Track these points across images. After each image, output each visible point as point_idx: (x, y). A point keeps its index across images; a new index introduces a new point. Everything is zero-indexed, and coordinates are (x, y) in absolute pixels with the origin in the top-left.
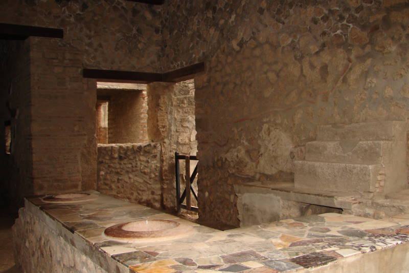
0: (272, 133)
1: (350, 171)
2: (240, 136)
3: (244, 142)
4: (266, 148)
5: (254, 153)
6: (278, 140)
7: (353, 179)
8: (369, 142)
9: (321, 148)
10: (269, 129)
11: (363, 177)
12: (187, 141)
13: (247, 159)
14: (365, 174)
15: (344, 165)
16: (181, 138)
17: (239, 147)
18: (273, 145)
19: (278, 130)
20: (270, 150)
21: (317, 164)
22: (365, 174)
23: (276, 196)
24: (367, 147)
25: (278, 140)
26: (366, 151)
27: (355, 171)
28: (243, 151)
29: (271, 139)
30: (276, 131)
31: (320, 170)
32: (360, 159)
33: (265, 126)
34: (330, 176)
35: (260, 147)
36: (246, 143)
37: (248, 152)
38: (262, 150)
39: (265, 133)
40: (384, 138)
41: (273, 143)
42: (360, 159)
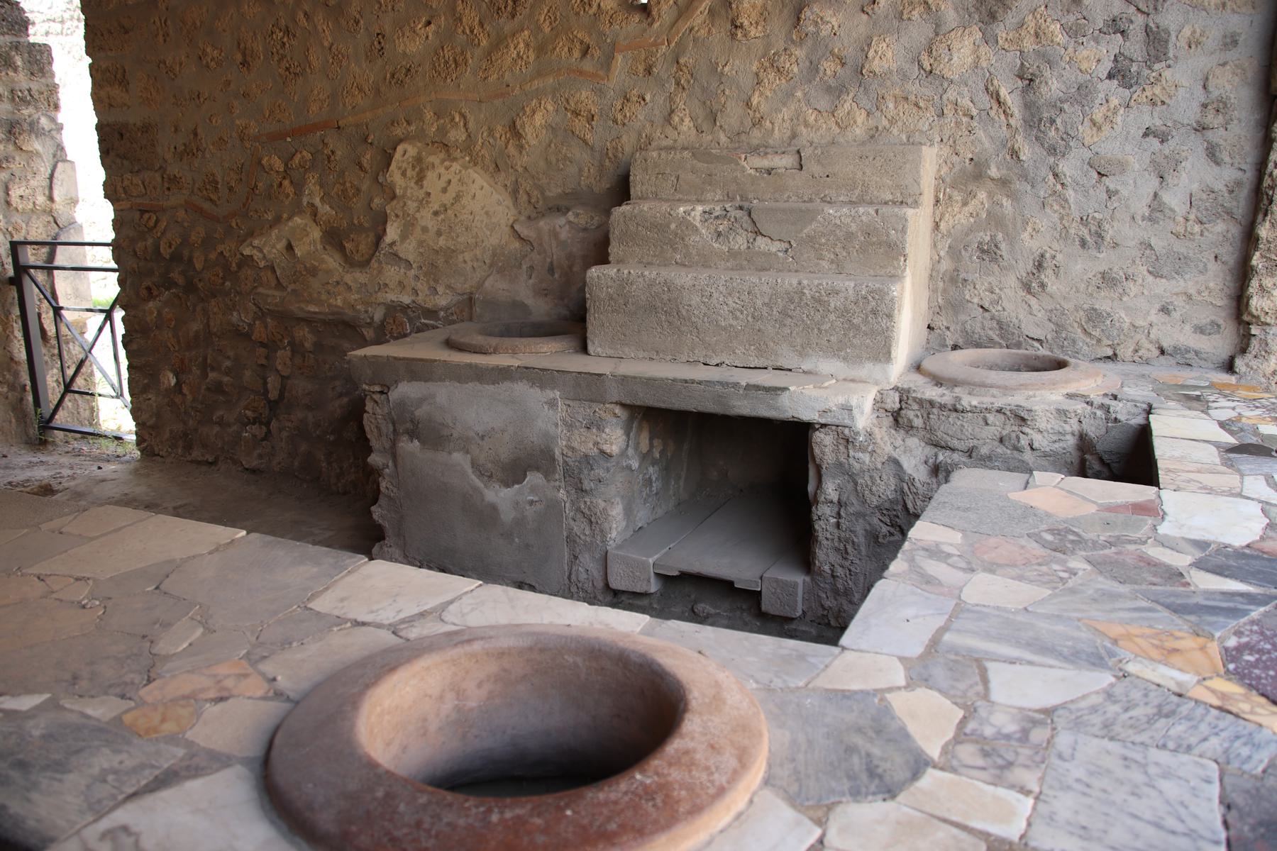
0: (431, 175)
1: (819, 301)
2: (299, 187)
3: (317, 201)
4: (409, 226)
5: (357, 237)
6: (458, 198)
7: (826, 327)
8: (861, 210)
9: (673, 226)
10: (419, 160)
11: (865, 321)
12: (41, 200)
13: (332, 261)
14: (874, 312)
15: (795, 282)
16: (20, 192)
17: (298, 220)
18: (436, 213)
19: (456, 166)
20: (425, 230)
21: (683, 278)
22: (874, 312)
23: (542, 387)
24: (854, 227)
25: (458, 198)
26: (850, 236)
27: (834, 302)
28: (316, 234)
29: (429, 194)
30: (447, 169)
31: (696, 300)
32: (825, 264)
33: (405, 153)
34: (737, 318)
35: (381, 221)
36: (325, 209)
37: (334, 238)
38: (392, 233)
39: (404, 174)
40: (891, 197)
41: (436, 207)
42: (825, 264)
